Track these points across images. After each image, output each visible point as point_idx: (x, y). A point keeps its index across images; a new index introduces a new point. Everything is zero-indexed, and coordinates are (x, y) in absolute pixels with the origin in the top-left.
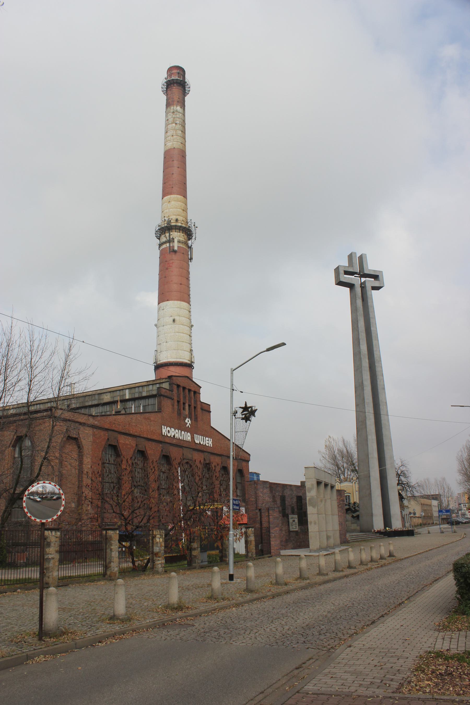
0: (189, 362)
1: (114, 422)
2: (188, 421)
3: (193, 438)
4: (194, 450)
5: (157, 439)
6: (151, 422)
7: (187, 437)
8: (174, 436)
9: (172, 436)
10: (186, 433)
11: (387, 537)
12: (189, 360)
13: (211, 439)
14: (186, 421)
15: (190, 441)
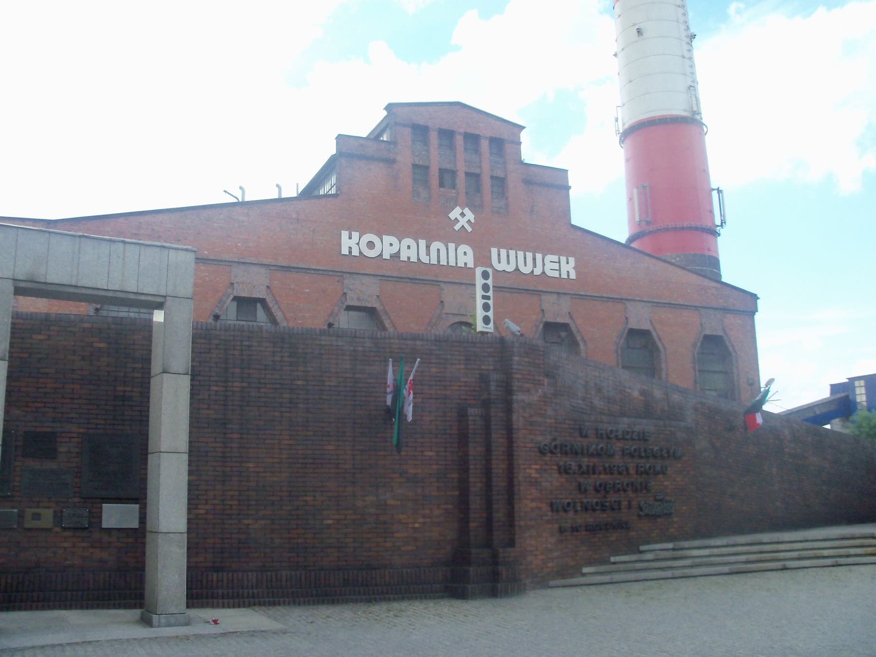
2: (463, 215)
8: (396, 256)
9: (386, 256)
10: (452, 246)
12: (685, 111)
13: (572, 260)
14: (455, 214)
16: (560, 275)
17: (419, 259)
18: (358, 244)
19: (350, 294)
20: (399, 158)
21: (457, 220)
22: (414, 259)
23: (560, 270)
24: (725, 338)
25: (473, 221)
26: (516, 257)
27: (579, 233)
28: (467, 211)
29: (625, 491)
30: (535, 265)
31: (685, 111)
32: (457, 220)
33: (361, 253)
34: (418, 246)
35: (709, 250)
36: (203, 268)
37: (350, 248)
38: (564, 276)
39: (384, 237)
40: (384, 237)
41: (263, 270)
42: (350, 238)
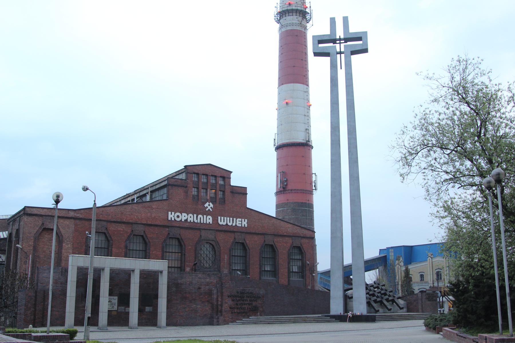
0: (304, 142)
1: (101, 213)
2: (209, 205)
3: (215, 220)
4: (217, 231)
5: (161, 224)
6: (152, 210)
7: (209, 220)
8: (186, 220)
9: (183, 220)
10: (205, 216)
11: (339, 321)
12: (303, 140)
13: (246, 220)
14: (206, 205)
15: (211, 223)
16: (242, 225)
17: (194, 221)
18: (174, 216)
19: (171, 234)
20: (189, 185)
21: (207, 207)
22: (192, 221)
23: (242, 224)
24: (301, 247)
25: (212, 207)
26: (227, 220)
27: (250, 210)
28: (211, 204)
29: (247, 305)
30: (233, 222)
31: (303, 140)
32: (207, 207)
33: (175, 219)
34: (194, 217)
35: (308, 200)
36: (123, 225)
37: (171, 218)
38: (243, 226)
39: (183, 214)
40: (183, 214)
41: (142, 226)
42: (171, 214)
